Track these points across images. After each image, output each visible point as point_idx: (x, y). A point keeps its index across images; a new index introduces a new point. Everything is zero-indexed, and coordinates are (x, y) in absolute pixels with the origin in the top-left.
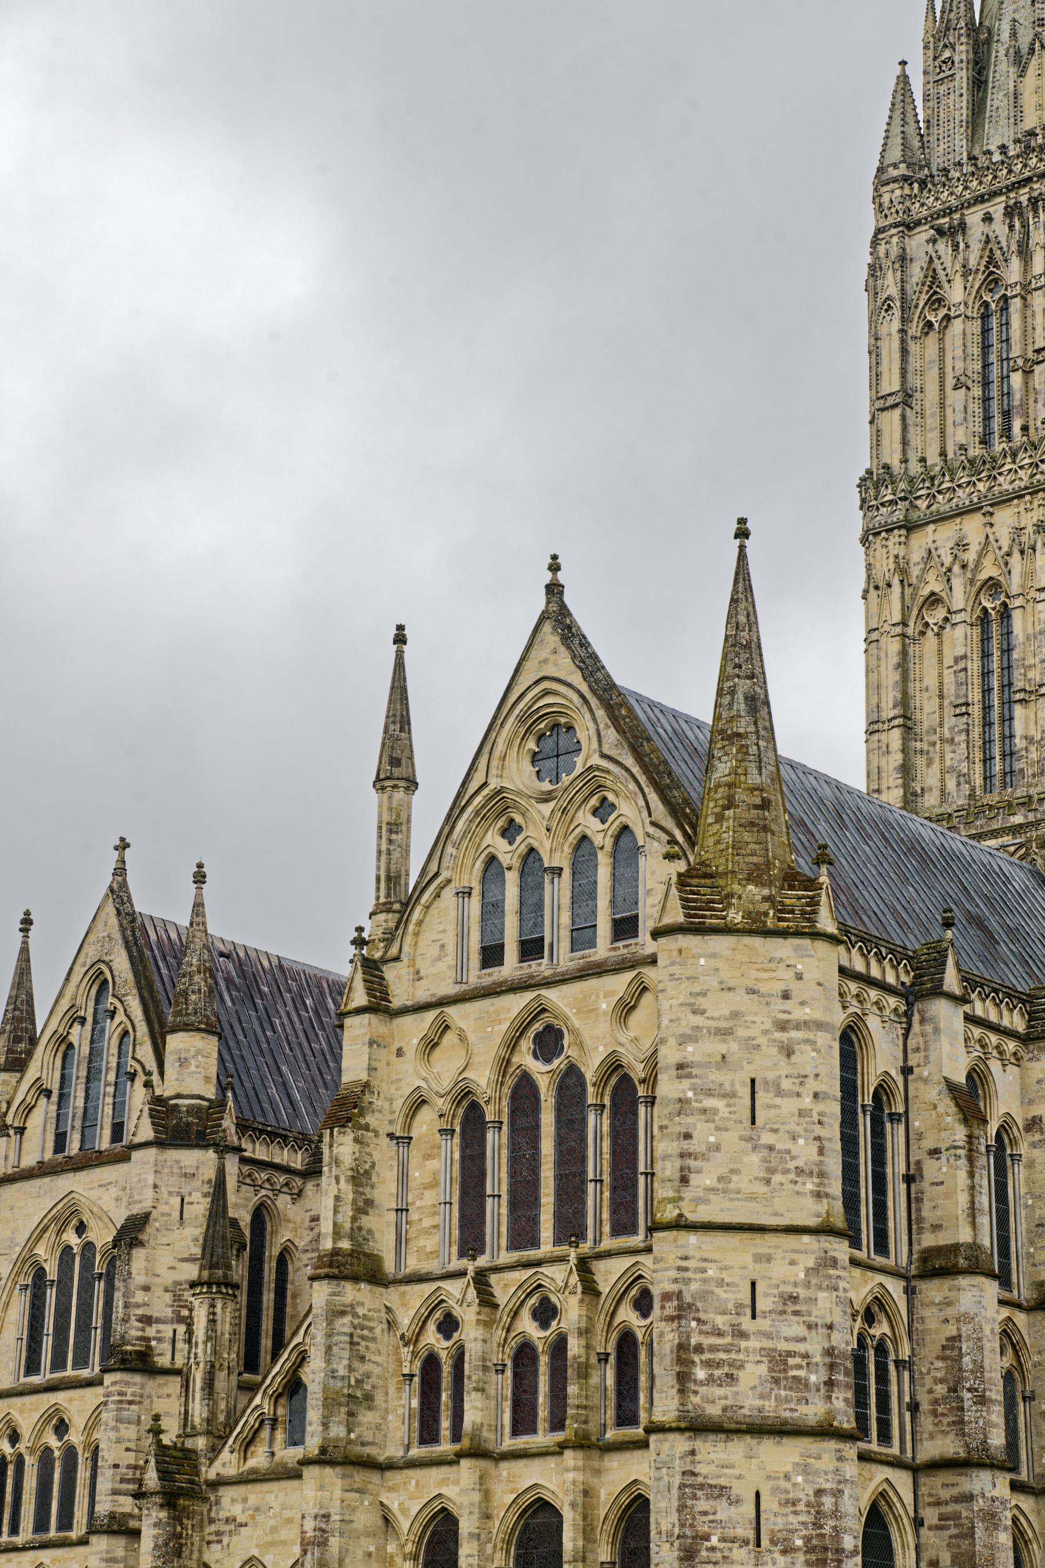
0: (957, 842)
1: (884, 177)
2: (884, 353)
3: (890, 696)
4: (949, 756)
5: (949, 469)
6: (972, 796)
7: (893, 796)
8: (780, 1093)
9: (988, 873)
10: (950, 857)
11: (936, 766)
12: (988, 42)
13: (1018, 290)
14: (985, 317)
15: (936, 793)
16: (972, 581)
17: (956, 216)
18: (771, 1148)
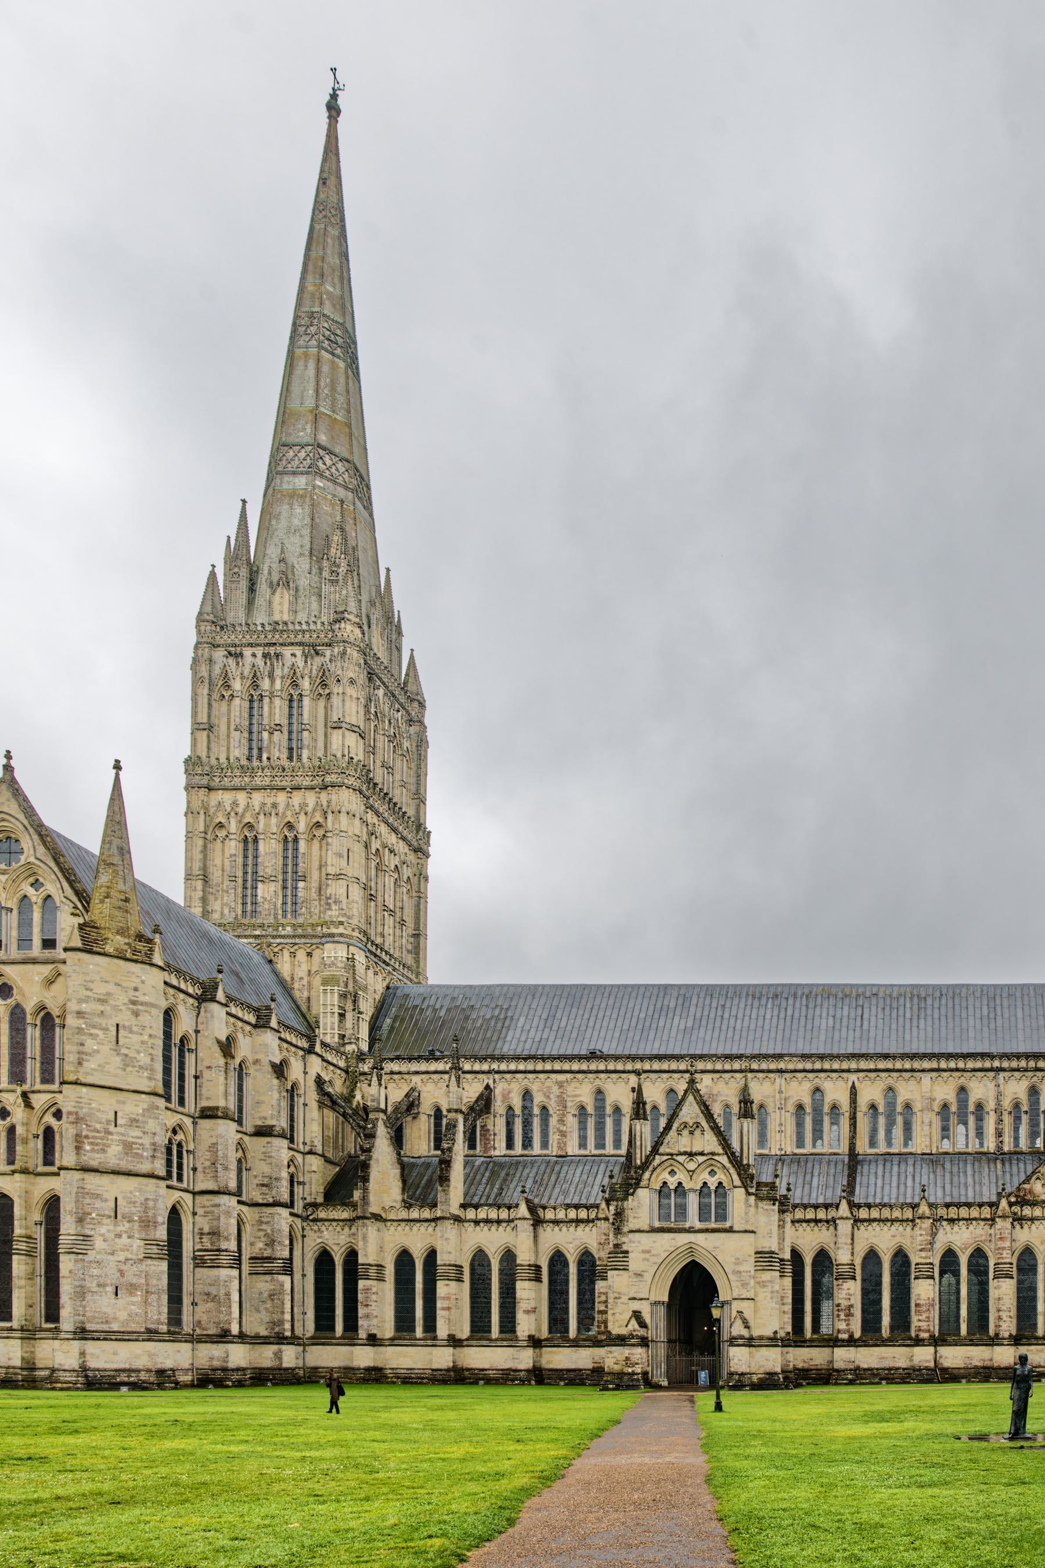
0: (228, 937)
1: (202, 618)
2: (200, 703)
3: (197, 866)
4: (226, 898)
5: (229, 766)
6: (236, 918)
7: (197, 911)
8: (131, 1032)
9: (242, 954)
10: (223, 944)
11: (219, 902)
12: (257, 572)
13: (267, 693)
14: (251, 701)
15: (219, 913)
16: (240, 822)
17: (239, 649)
18: (126, 1055)
